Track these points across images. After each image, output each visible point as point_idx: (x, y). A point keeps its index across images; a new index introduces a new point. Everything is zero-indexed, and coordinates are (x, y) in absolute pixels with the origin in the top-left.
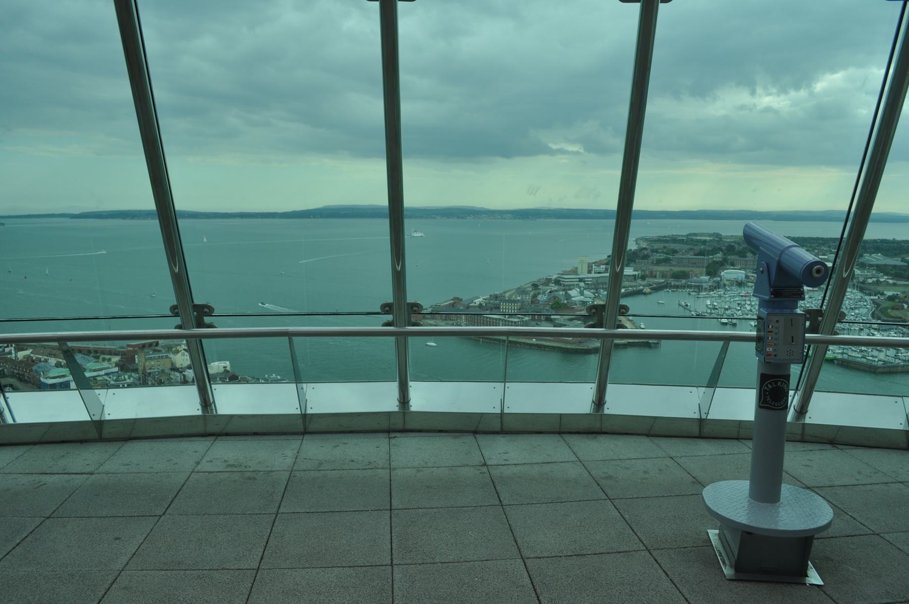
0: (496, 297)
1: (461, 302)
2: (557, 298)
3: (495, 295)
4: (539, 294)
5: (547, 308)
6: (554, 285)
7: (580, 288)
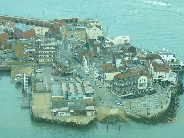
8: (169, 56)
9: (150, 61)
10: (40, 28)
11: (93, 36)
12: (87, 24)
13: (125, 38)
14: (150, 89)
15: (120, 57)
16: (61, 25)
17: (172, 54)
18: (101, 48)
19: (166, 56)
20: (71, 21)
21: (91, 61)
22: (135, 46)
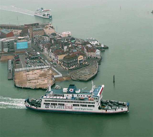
10: (16, 30)
11: (49, 33)
12: (44, 26)
14: (85, 63)
15: (66, 45)
16: (28, 28)
17: (96, 40)
18: (54, 40)
19: (93, 42)
21: (49, 49)
22: (74, 37)
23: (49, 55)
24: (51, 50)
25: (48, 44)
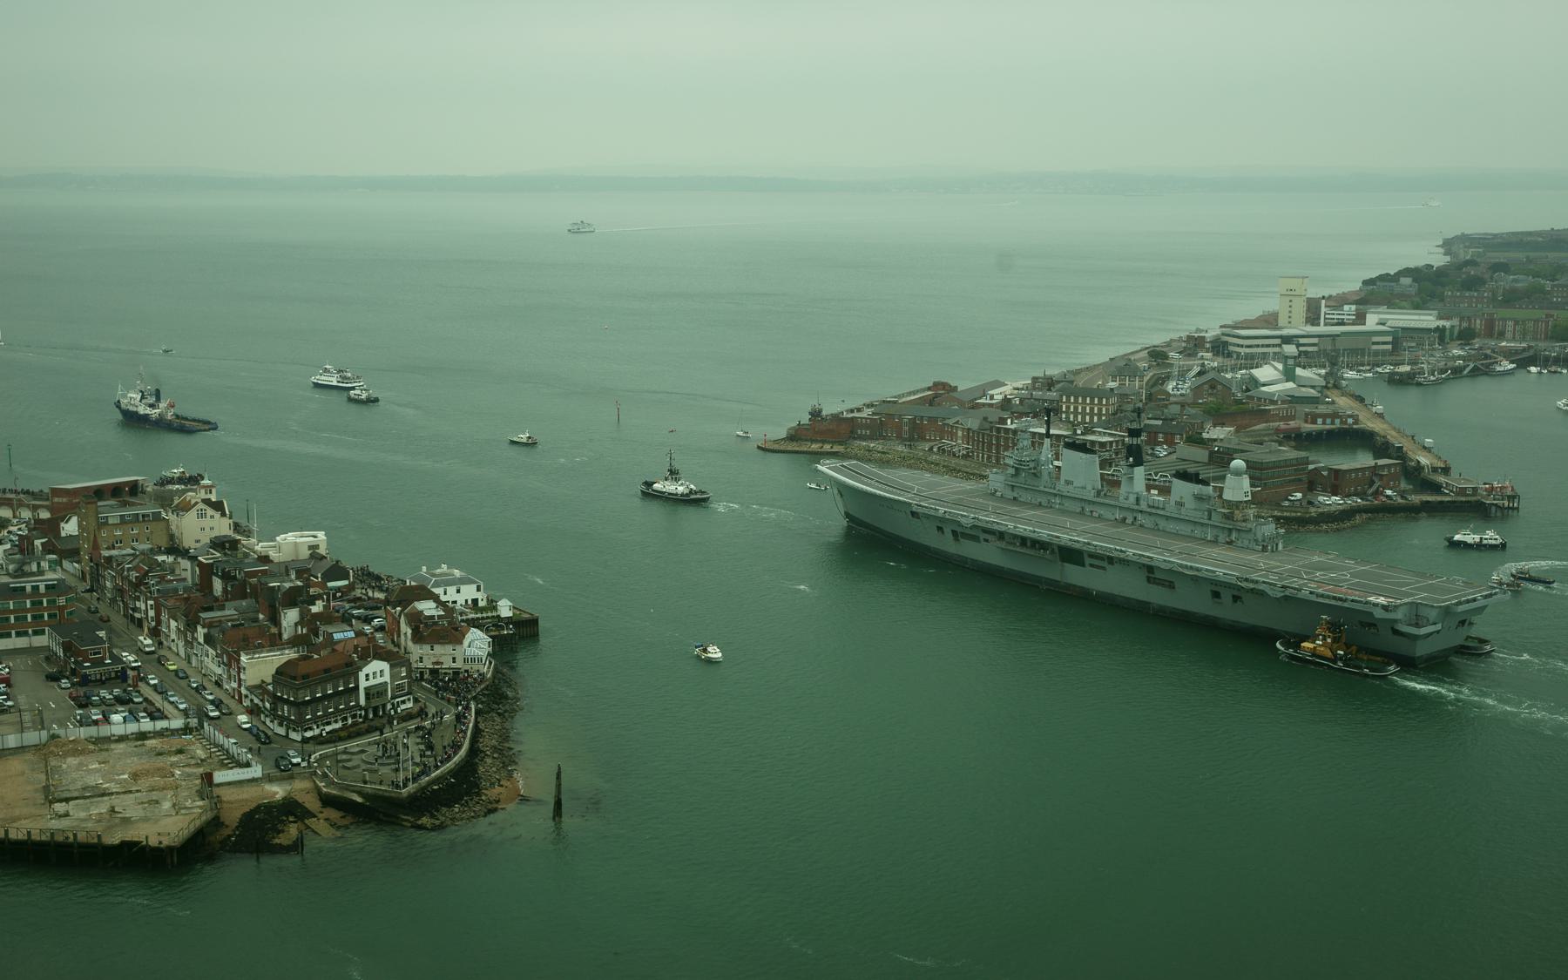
0: (1050, 383)
1: (954, 394)
2: (1219, 387)
3: (1045, 377)
4: (1168, 377)
5: (1193, 411)
6: (1209, 355)
7: (1284, 358)
8: (463, 588)
9: (399, 609)
13: (312, 539)
14: (403, 702)
17: (473, 582)
18: (226, 577)
19: (452, 590)
20: (116, 491)
21: (191, 625)
23: (189, 662)
24: (201, 632)
25: (187, 599)
